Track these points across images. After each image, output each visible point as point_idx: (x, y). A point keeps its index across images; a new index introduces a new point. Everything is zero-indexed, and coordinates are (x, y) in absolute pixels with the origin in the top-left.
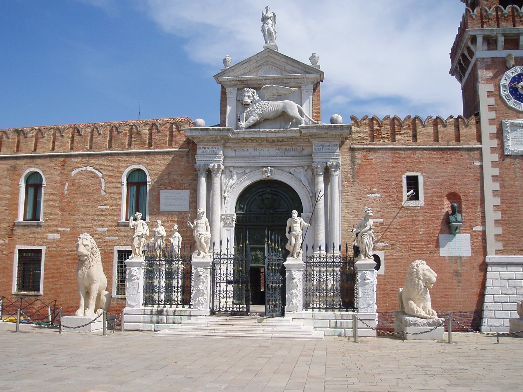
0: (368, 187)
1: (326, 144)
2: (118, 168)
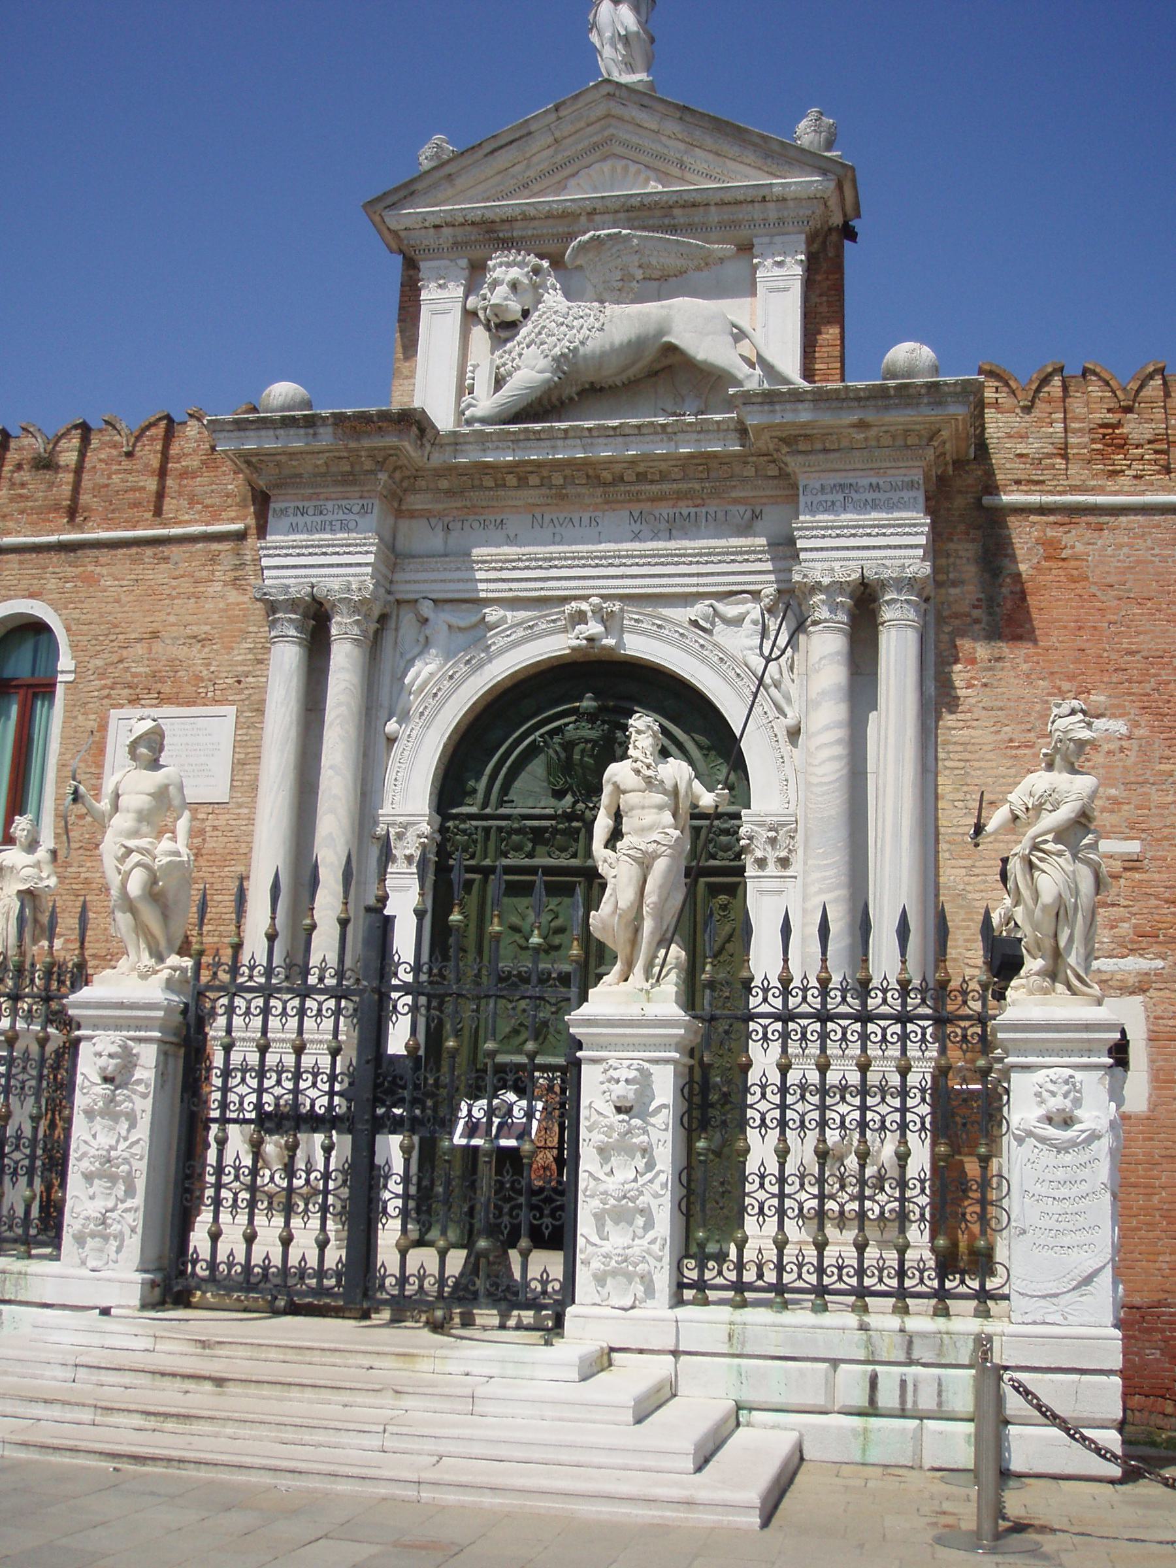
0: (1066, 686)
1: (865, 482)
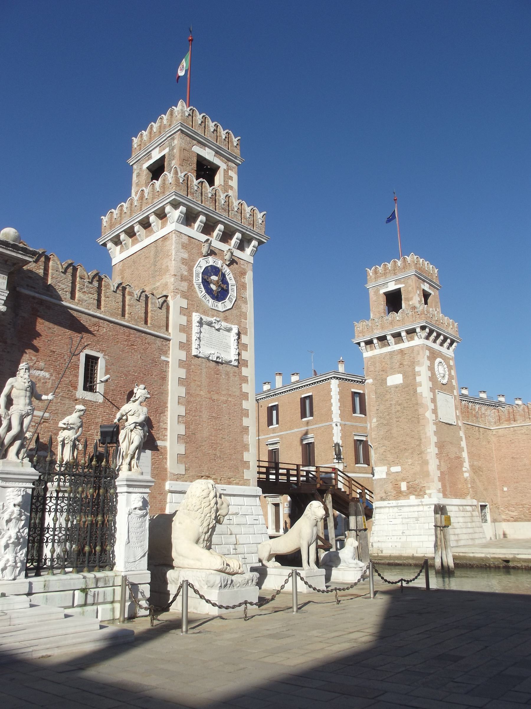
0: (33, 358)
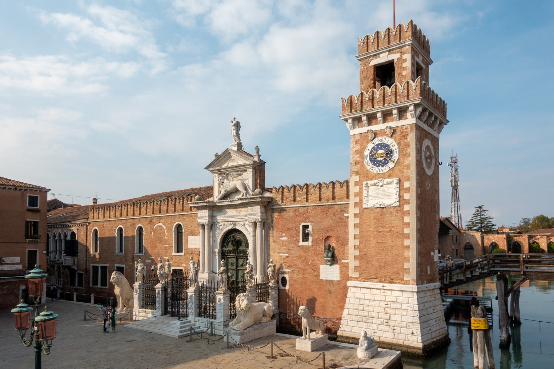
2: (171, 223)
